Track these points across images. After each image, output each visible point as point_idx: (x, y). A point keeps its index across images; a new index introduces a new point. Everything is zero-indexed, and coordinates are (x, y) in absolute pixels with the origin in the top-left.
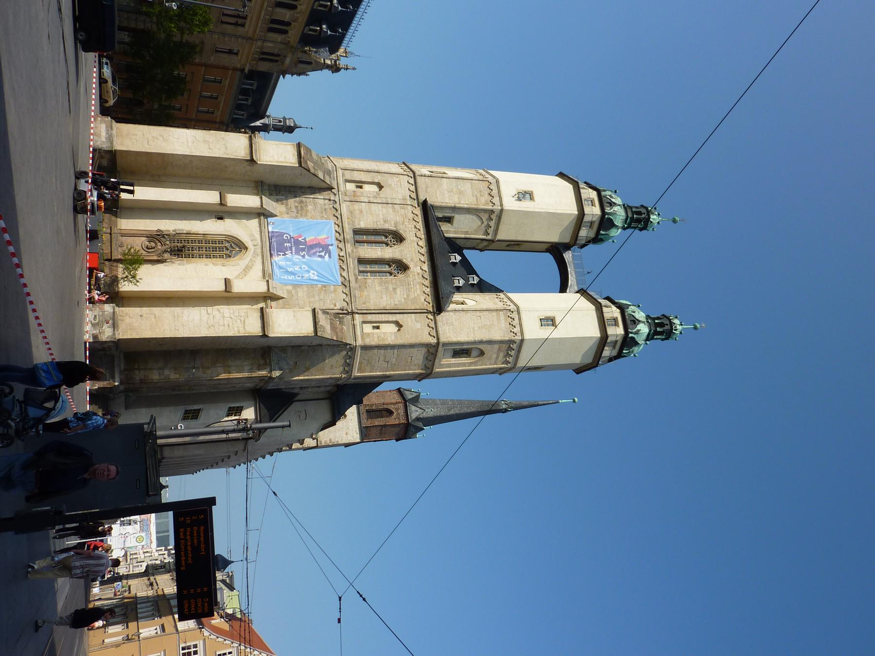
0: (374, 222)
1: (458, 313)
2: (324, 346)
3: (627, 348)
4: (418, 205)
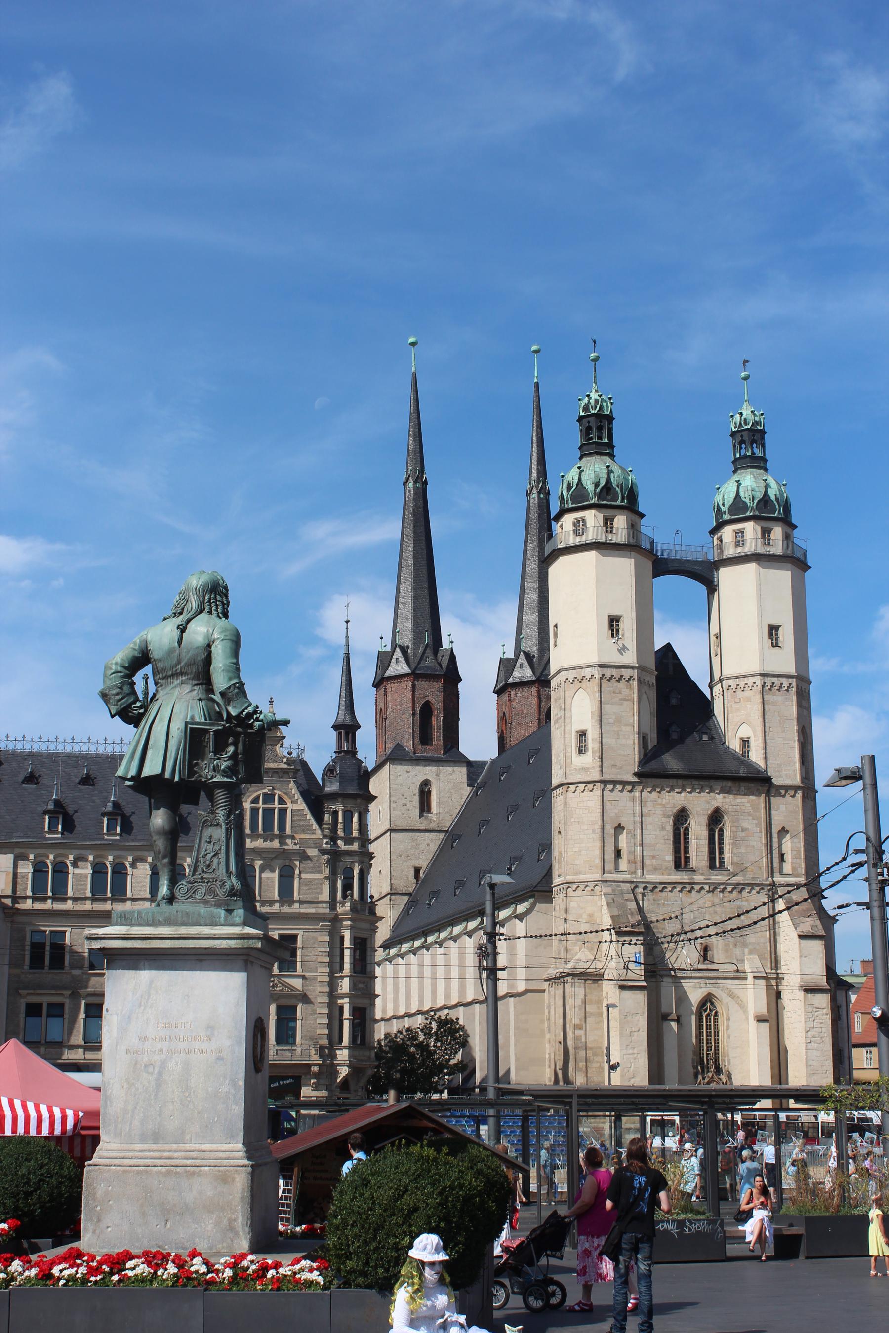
0: (665, 843)
1: (768, 756)
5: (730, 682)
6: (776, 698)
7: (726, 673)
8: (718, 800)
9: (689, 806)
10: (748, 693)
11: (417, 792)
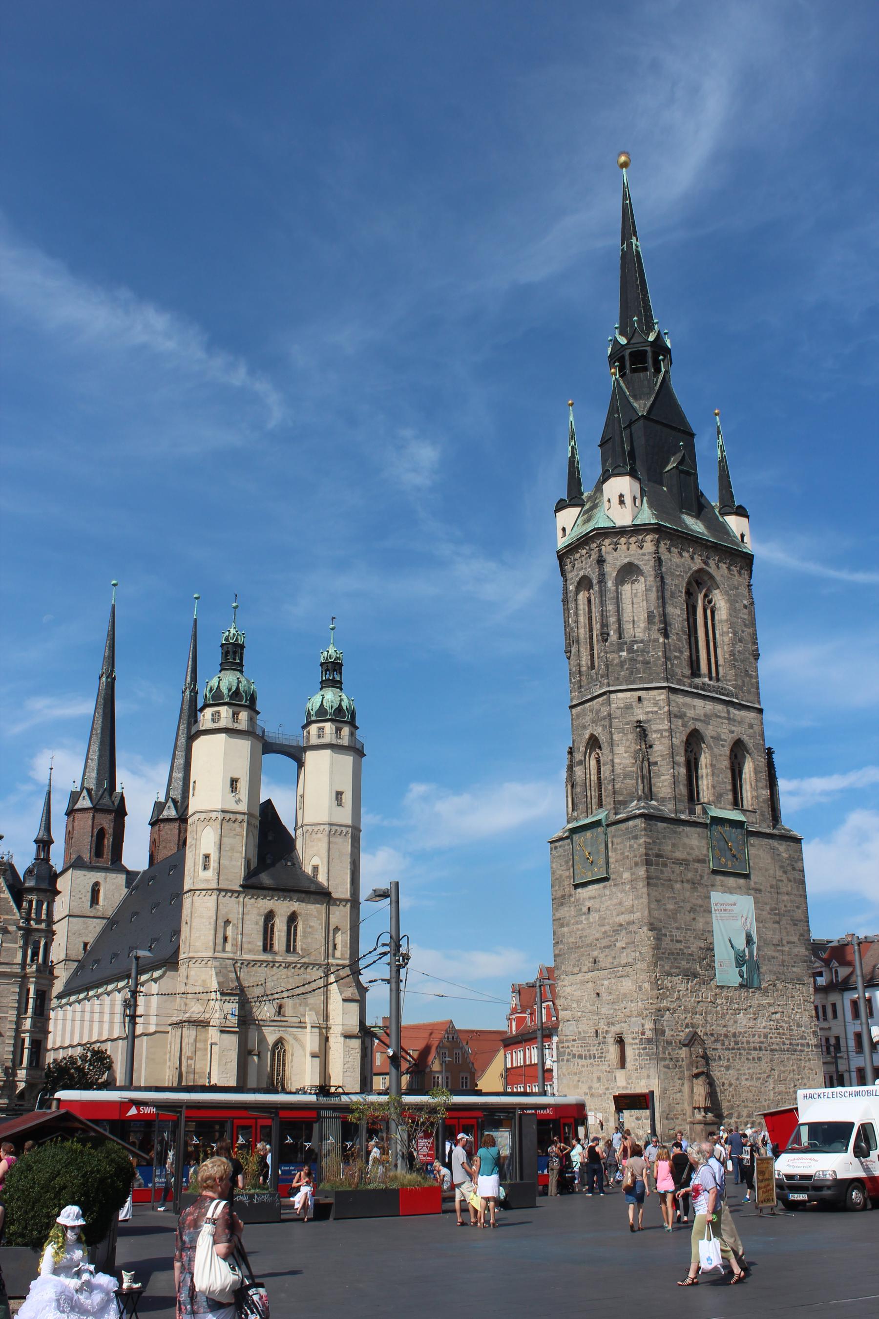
5: (308, 828)
6: (338, 840)
7: (306, 821)
9: (276, 910)
10: (319, 835)
11: (90, 890)
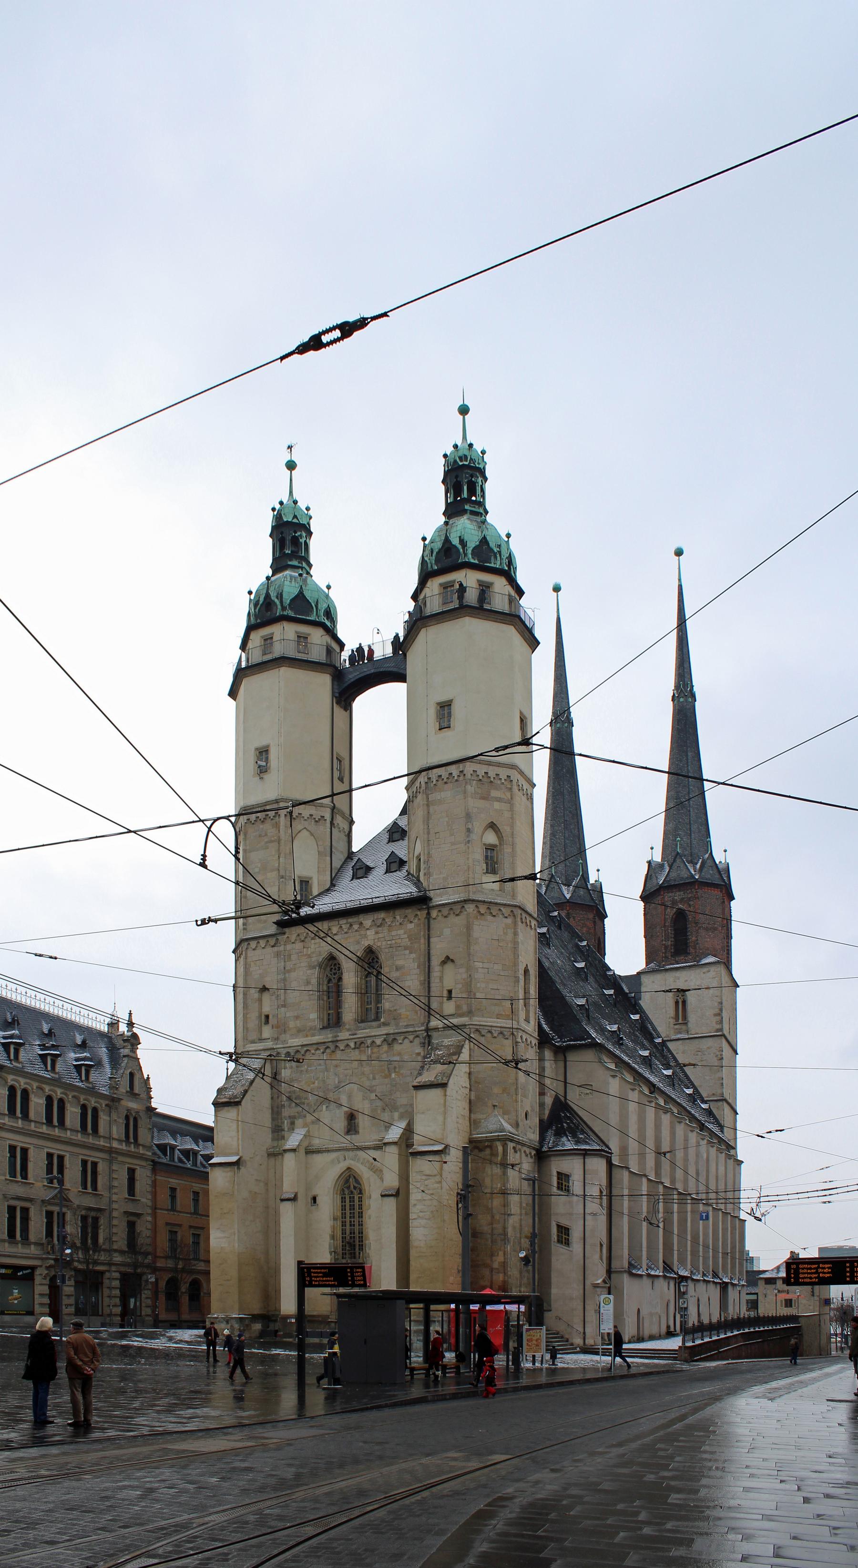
2: (472, 1070)
3: (492, 558)
4: (284, 933)
8: (369, 938)
